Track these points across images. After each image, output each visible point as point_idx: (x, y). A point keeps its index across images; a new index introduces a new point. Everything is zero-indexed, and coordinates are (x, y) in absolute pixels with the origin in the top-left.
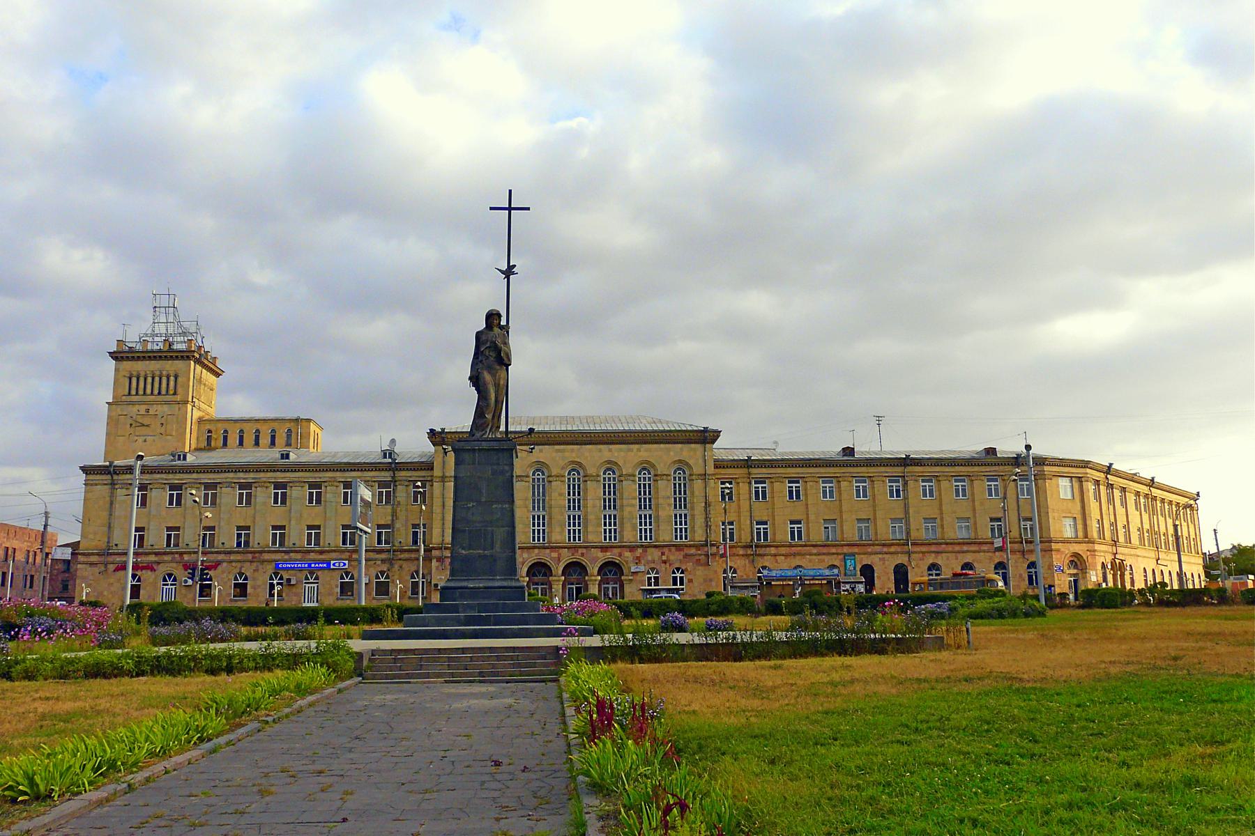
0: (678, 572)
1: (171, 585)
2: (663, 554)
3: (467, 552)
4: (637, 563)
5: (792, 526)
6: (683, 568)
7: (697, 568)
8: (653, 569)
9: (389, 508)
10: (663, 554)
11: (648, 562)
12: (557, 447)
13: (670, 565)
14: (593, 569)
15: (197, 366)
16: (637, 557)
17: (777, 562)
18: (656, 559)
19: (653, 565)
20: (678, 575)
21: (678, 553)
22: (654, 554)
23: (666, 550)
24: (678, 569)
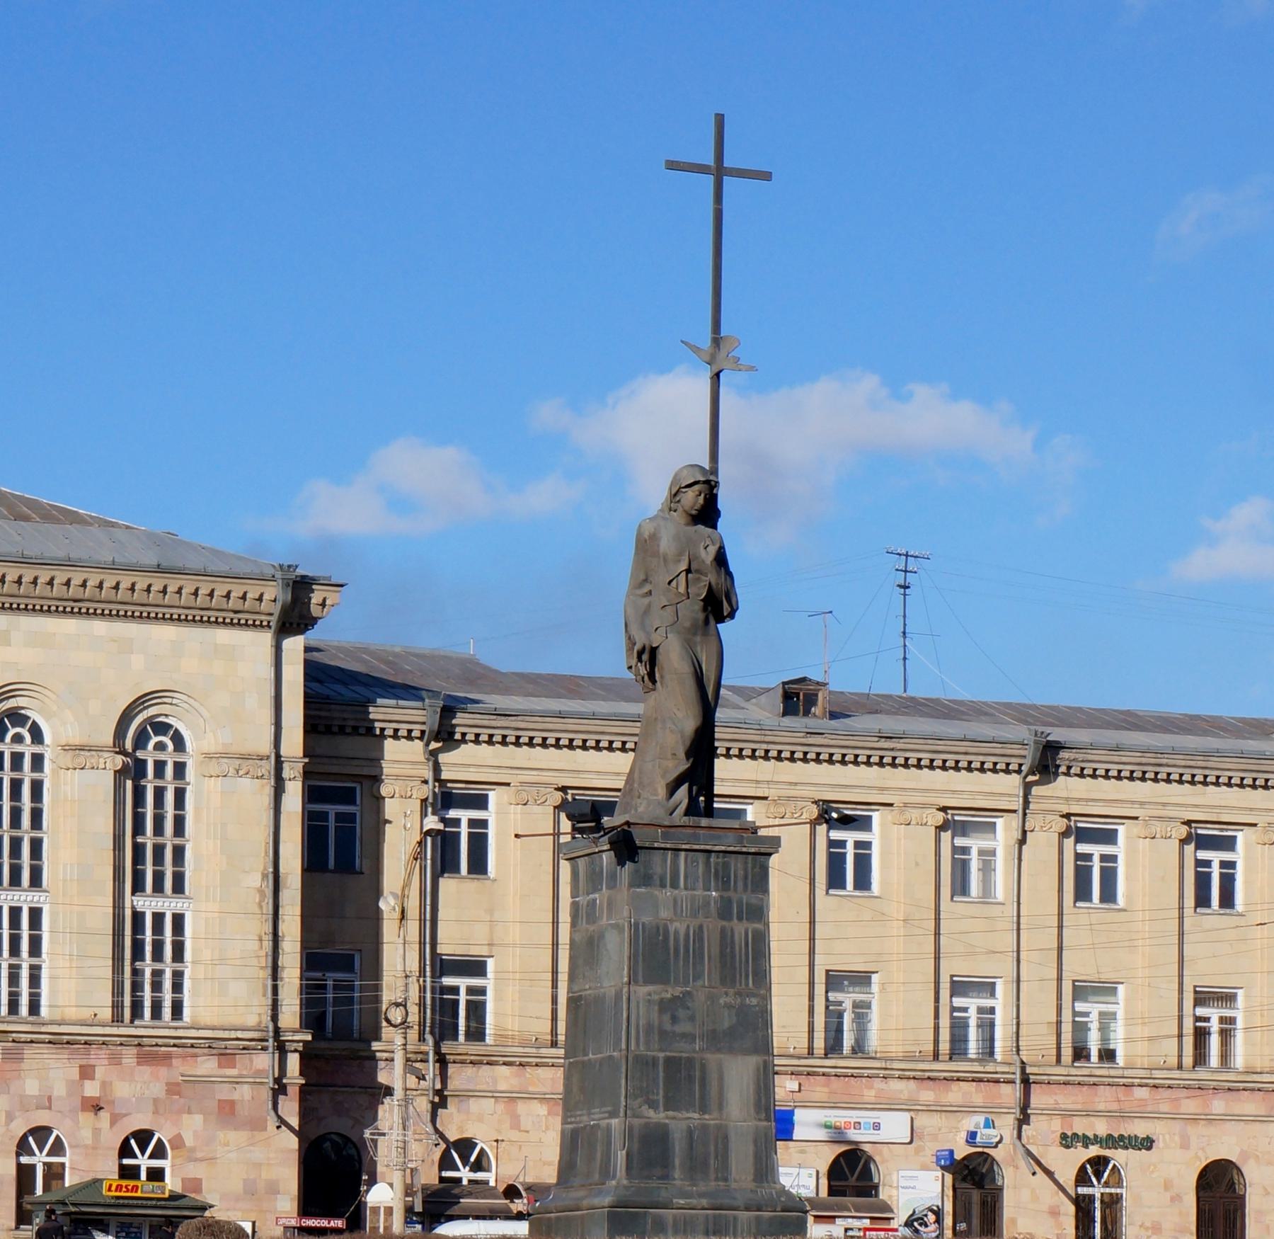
0: (143, 1153)
2: (87, 1072)
7: (221, 1135)
10: (87, 1072)
13: (114, 1120)
18: (60, 1090)
19: (42, 1119)
21: (146, 1071)
23: (98, 1059)
24: (143, 1137)
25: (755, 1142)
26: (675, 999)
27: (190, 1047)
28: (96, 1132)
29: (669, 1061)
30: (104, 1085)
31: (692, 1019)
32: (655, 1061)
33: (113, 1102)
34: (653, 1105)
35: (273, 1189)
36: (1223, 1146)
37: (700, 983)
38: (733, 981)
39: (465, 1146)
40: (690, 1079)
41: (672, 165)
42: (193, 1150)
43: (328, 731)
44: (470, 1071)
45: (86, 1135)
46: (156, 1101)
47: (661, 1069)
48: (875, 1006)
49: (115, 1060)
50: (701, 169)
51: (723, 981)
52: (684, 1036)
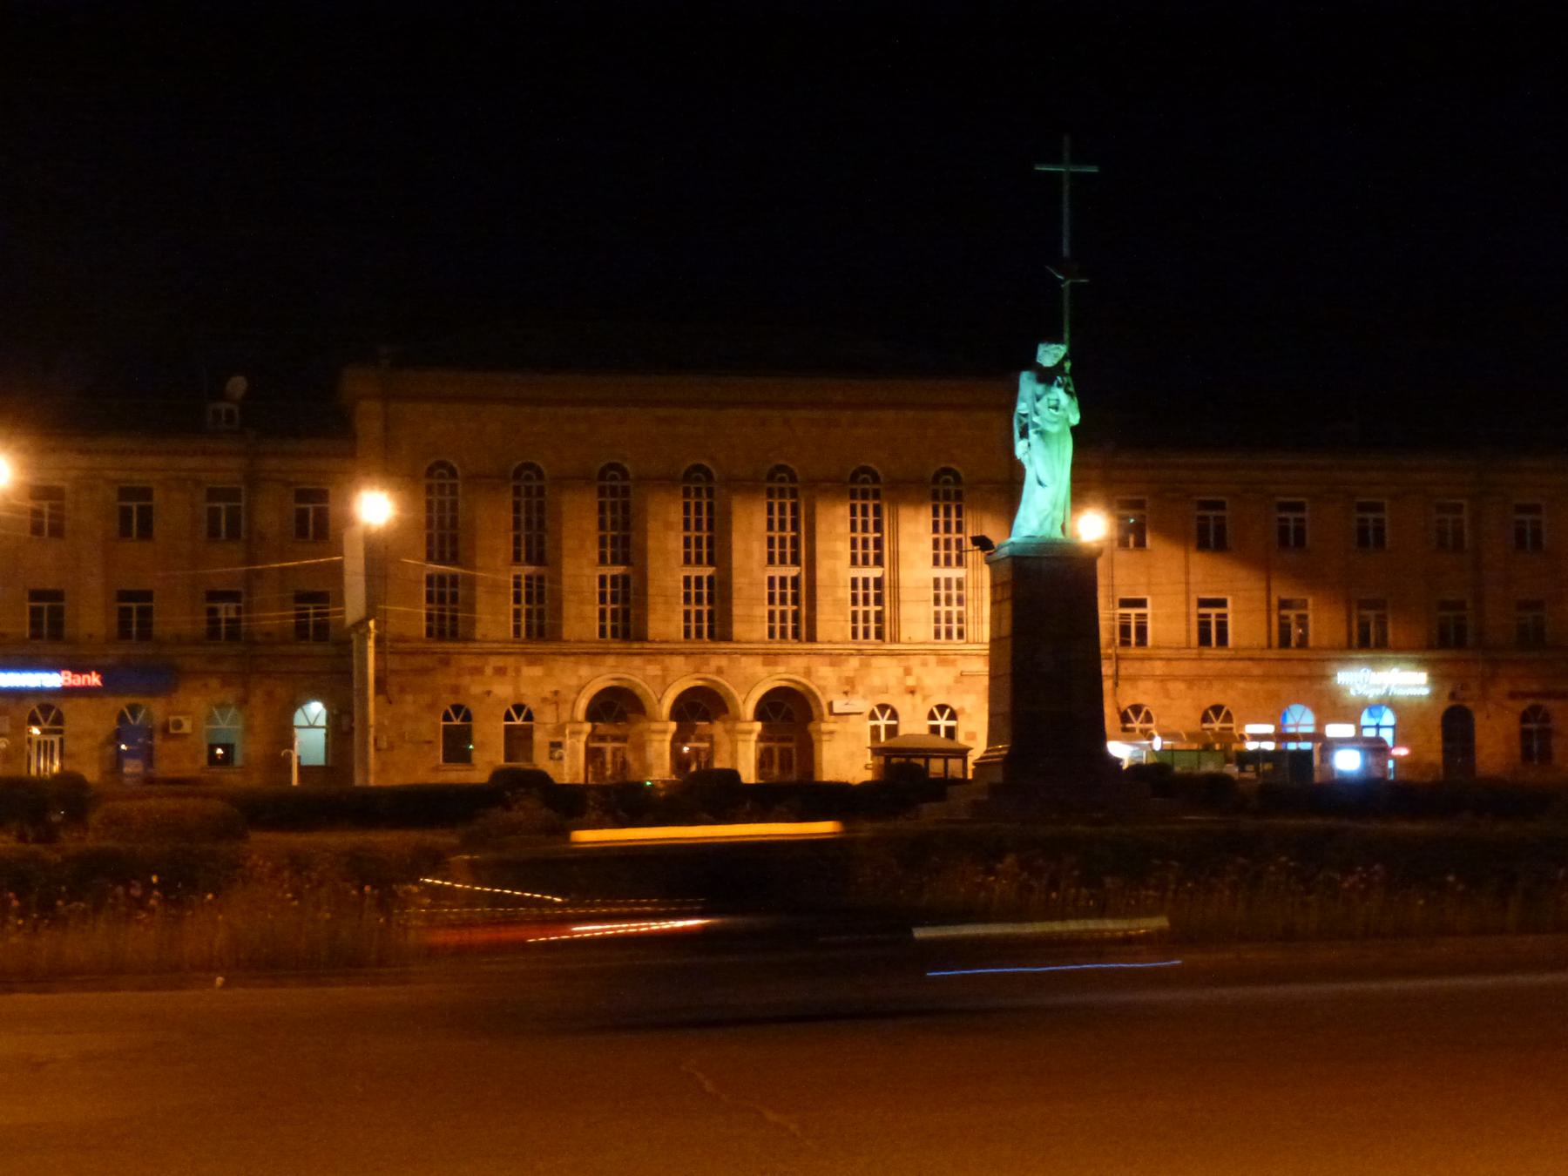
4: (846, 693)
5: (1204, 611)
6: (955, 706)
8: (883, 708)
10: (908, 672)
11: (873, 691)
12: (661, 412)
13: (925, 698)
18: (892, 682)
20: (943, 722)
28: (914, 707)
33: (922, 689)
39: (1137, 709)
42: (969, 715)
49: (924, 664)
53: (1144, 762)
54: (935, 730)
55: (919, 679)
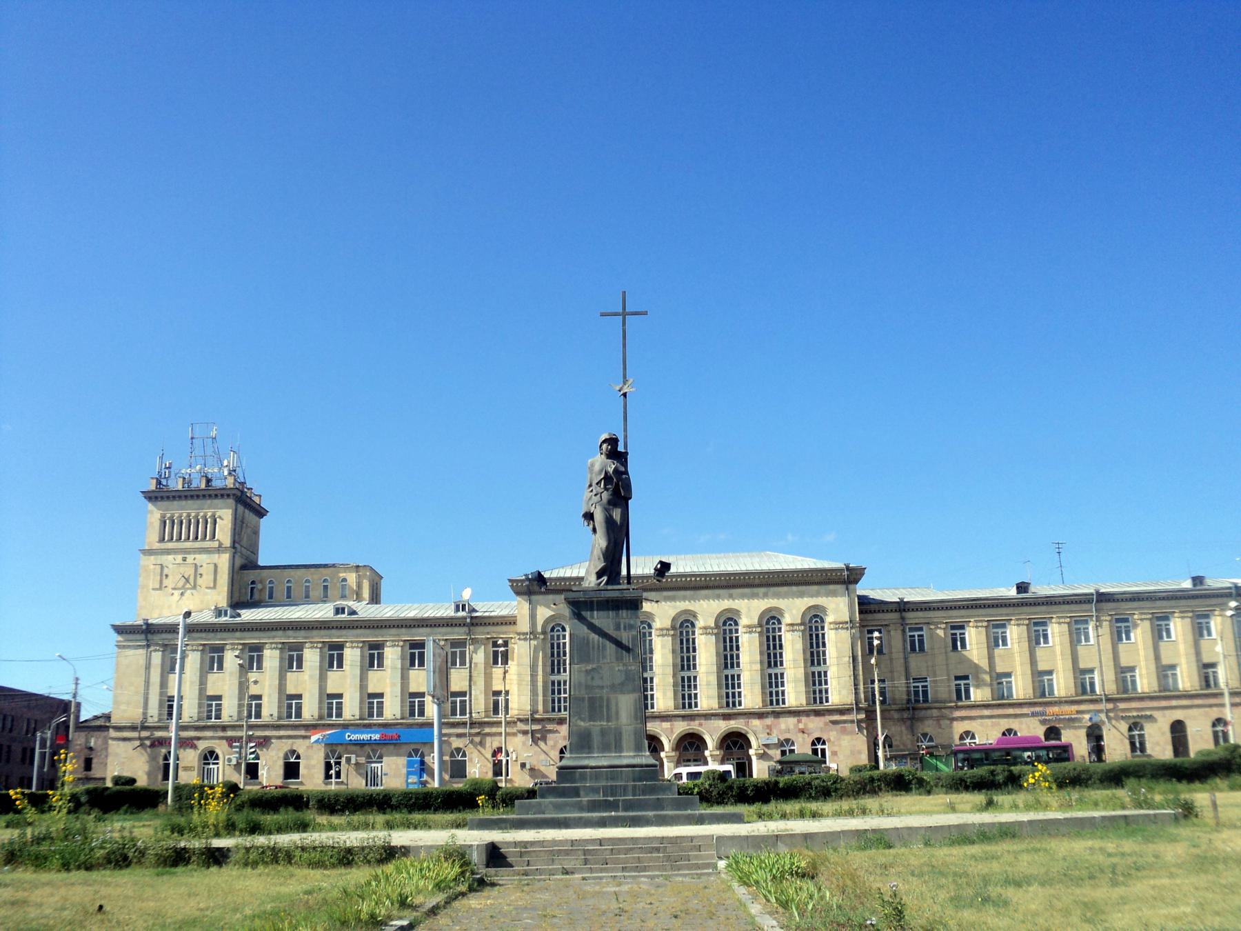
1: (214, 764)
3: (588, 724)
5: (958, 682)
6: (825, 737)
7: (843, 737)
8: (787, 740)
9: (465, 673)
10: (799, 721)
11: (781, 732)
14: (711, 742)
15: (239, 505)
16: (767, 726)
17: (940, 726)
18: (792, 727)
19: (788, 736)
20: (819, 747)
22: (788, 723)
24: (819, 740)
25: (635, 734)
26: (593, 669)
27: (831, 712)
28: (803, 738)
29: (589, 698)
30: (806, 724)
31: (602, 678)
32: (583, 699)
34: (581, 719)
35: (860, 752)
36: (1178, 715)
37: (605, 661)
38: (622, 659)
40: (601, 707)
41: (603, 315)
42: (833, 742)
43: (866, 612)
44: (924, 712)
45: (800, 740)
46: (821, 728)
47: (586, 702)
48: (1013, 683)
50: (616, 314)
51: (617, 659)
52: (598, 687)
53: (477, 777)
54: (815, 752)
55: (806, 724)
